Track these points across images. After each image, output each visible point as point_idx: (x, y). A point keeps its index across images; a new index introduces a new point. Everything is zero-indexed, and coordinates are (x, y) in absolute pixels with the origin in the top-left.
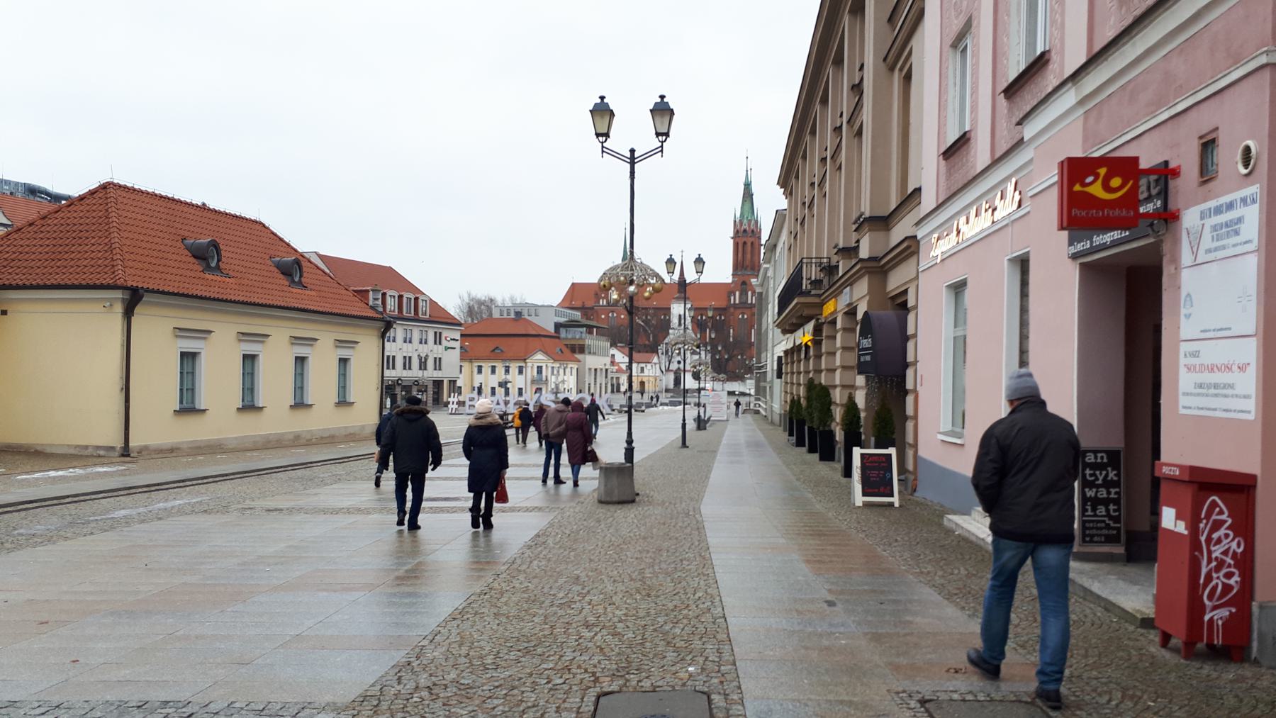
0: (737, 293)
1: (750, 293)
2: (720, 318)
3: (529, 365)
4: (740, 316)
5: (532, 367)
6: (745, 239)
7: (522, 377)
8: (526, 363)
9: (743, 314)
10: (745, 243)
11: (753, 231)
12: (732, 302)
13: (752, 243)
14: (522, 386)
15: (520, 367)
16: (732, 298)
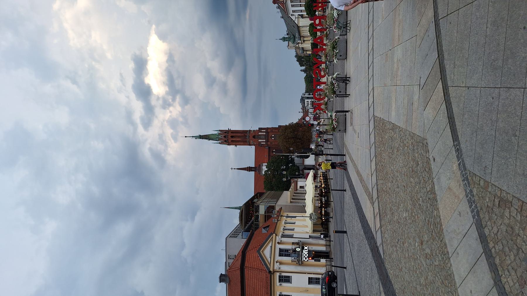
0: (259, 141)
1: (259, 133)
2: (274, 152)
3: (277, 266)
4: (273, 139)
5: (281, 263)
6: (229, 137)
7: (294, 277)
8: (274, 272)
9: (271, 137)
10: (232, 137)
11: (225, 133)
12: (265, 143)
13: (232, 133)
14: (306, 277)
15: (280, 281)
16: (262, 143)
